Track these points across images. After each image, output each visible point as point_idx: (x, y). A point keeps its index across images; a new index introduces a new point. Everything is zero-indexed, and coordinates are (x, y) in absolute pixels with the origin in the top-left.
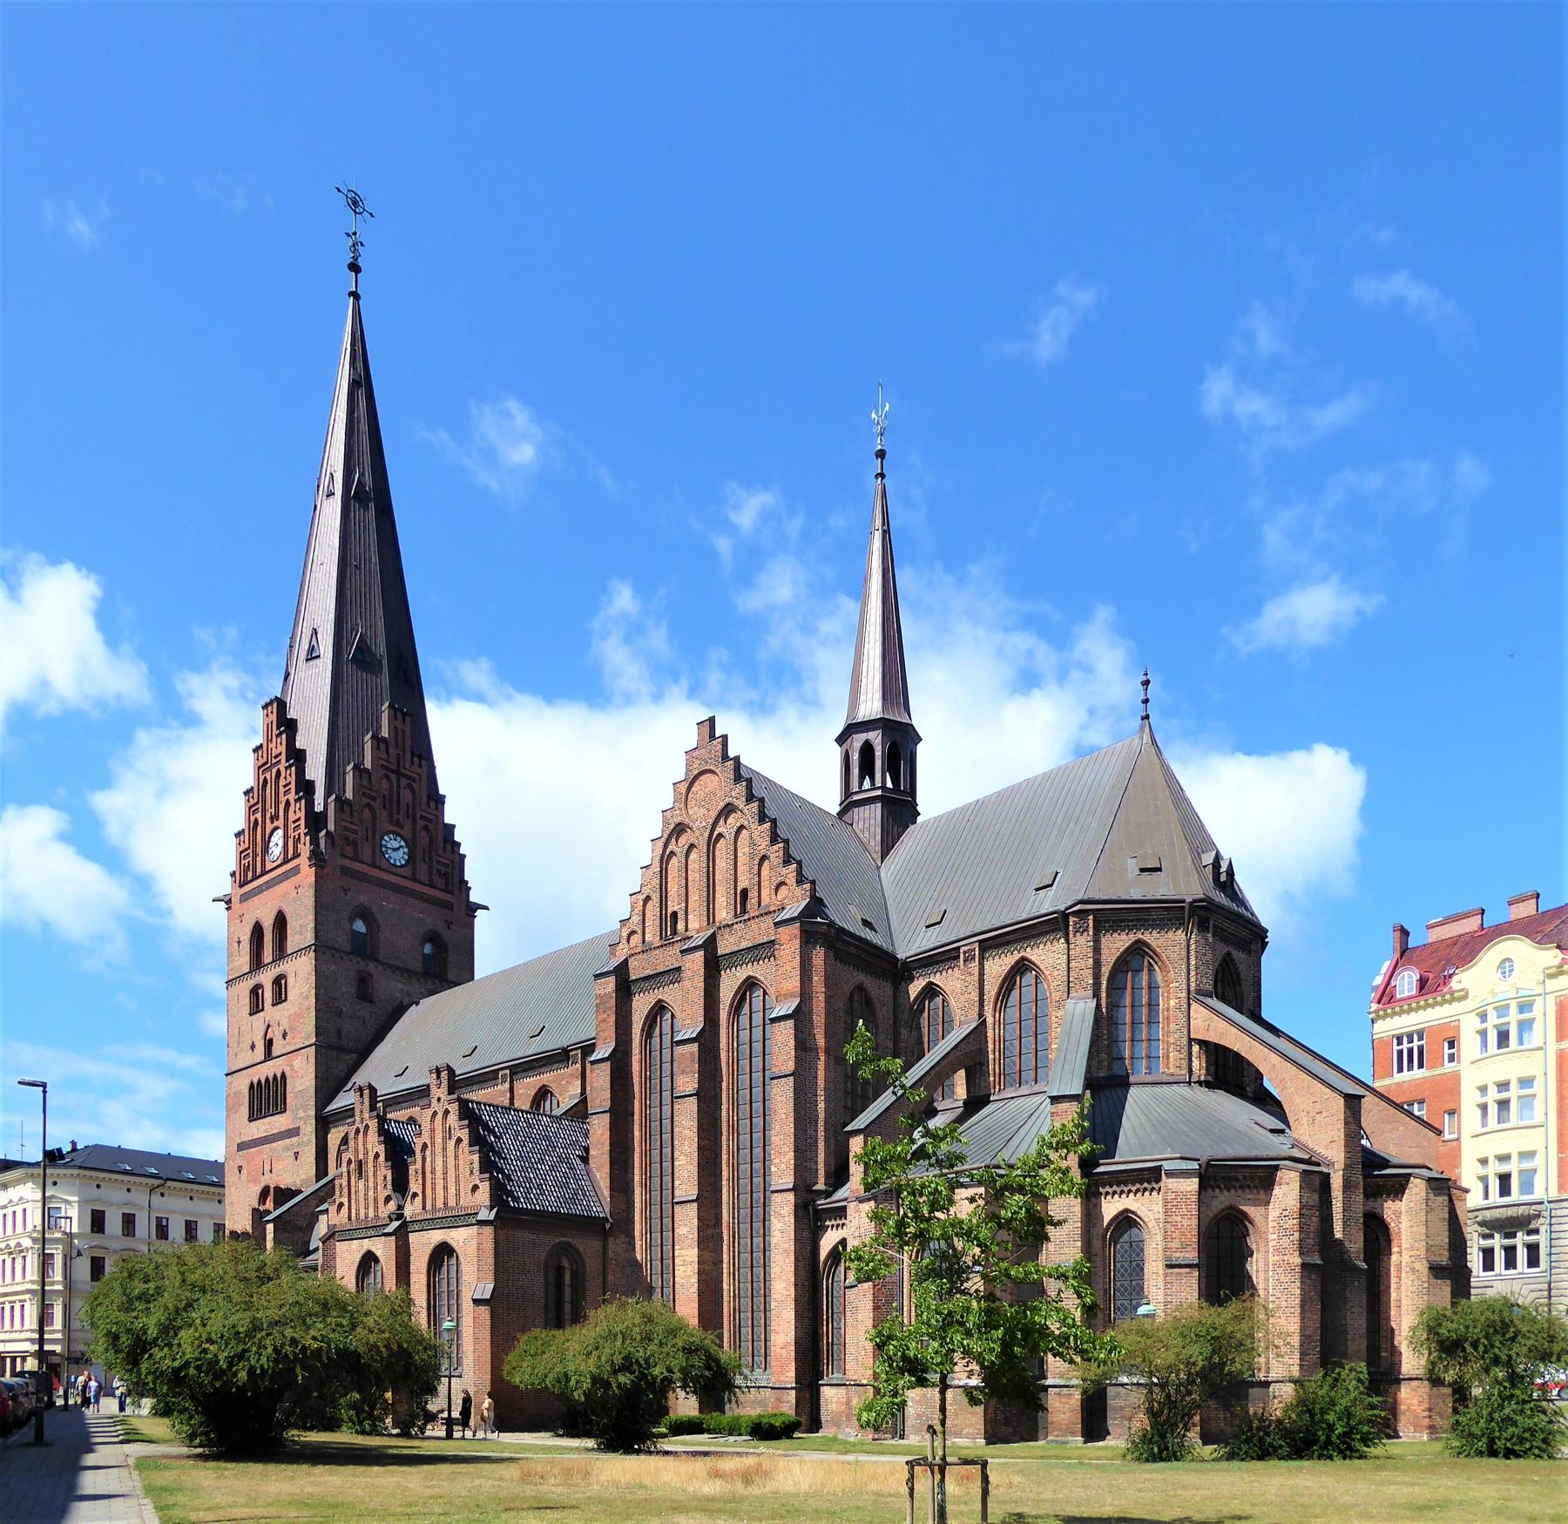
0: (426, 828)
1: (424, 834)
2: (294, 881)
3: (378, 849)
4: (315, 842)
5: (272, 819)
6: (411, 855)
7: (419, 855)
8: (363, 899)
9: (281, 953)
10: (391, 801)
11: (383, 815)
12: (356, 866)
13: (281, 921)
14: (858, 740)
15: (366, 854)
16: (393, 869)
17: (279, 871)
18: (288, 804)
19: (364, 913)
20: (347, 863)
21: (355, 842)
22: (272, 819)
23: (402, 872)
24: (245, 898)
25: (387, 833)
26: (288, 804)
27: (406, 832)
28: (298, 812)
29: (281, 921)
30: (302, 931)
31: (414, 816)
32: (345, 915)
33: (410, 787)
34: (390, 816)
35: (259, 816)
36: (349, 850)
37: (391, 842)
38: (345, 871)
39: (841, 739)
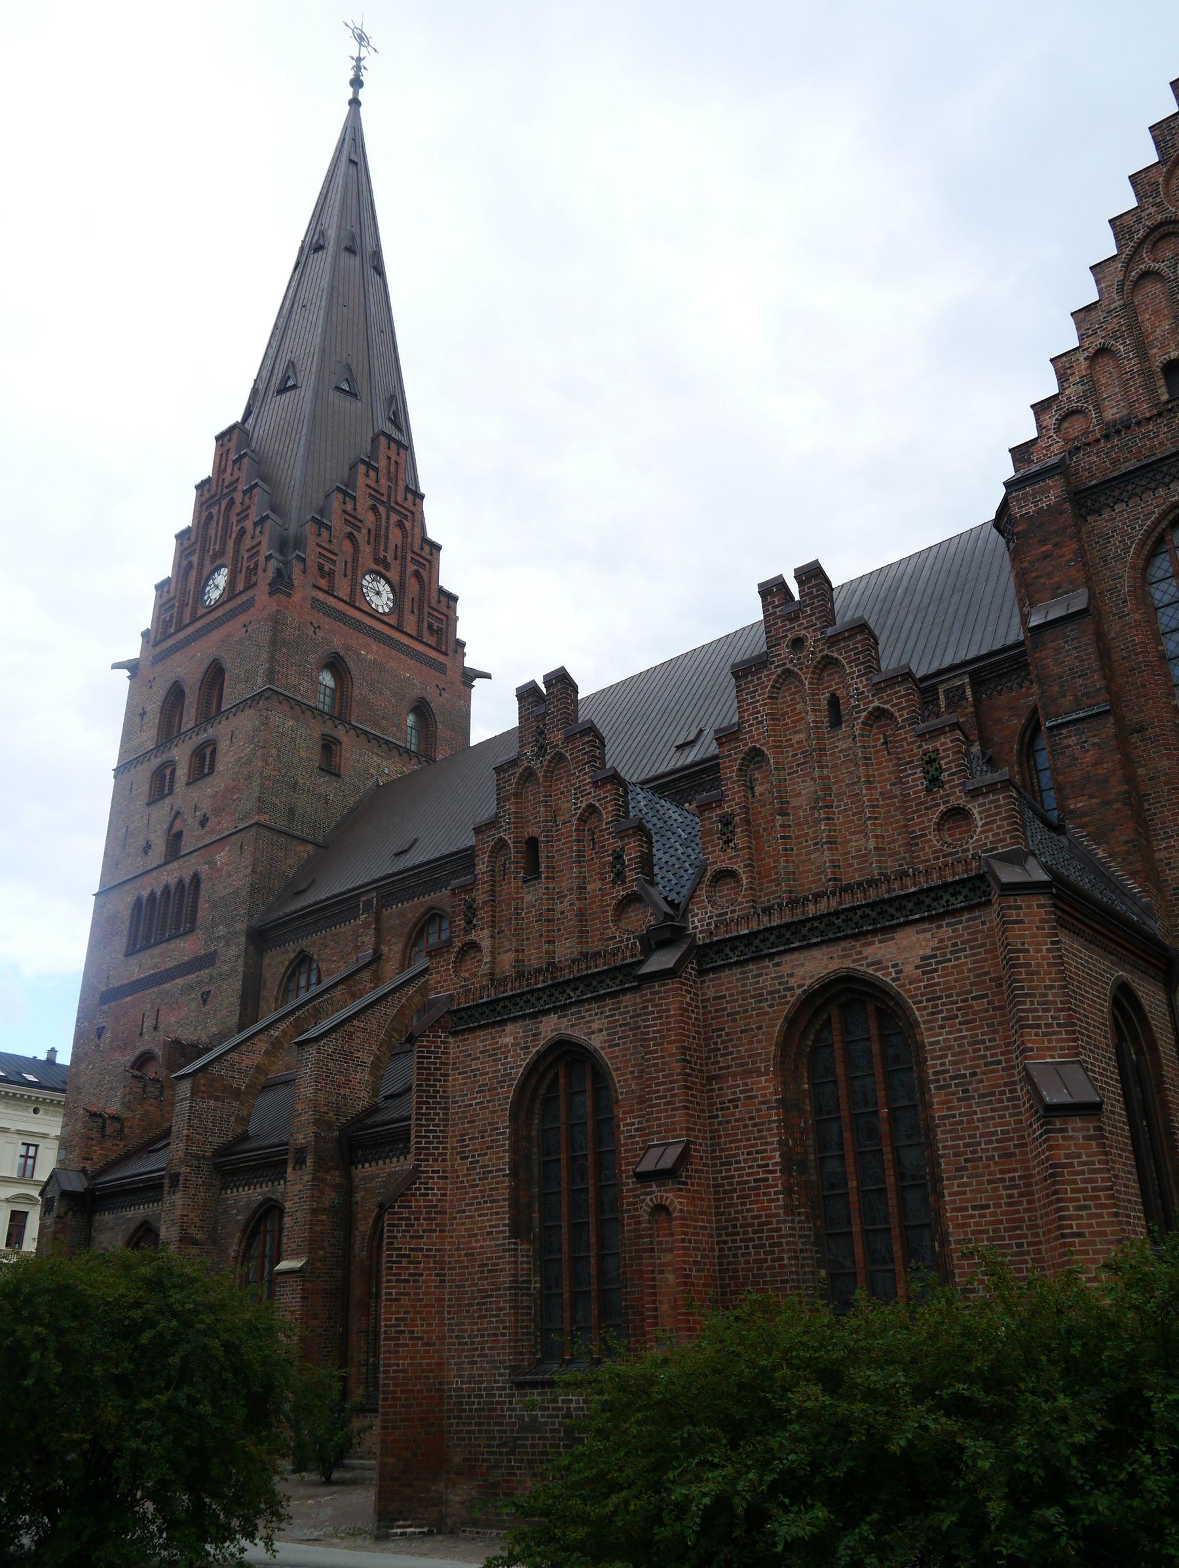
0: (417, 574)
1: (413, 581)
3: (356, 588)
7: (408, 605)
8: (337, 643)
10: (377, 536)
11: (366, 550)
12: (331, 601)
15: (343, 591)
16: (374, 615)
17: (219, 612)
19: (335, 664)
20: (320, 596)
21: (330, 575)
23: (386, 619)
25: (371, 572)
27: (393, 575)
31: (404, 558)
32: (312, 658)
33: (400, 525)
34: (376, 550)
36: (323, 583)
38: (316, 604)
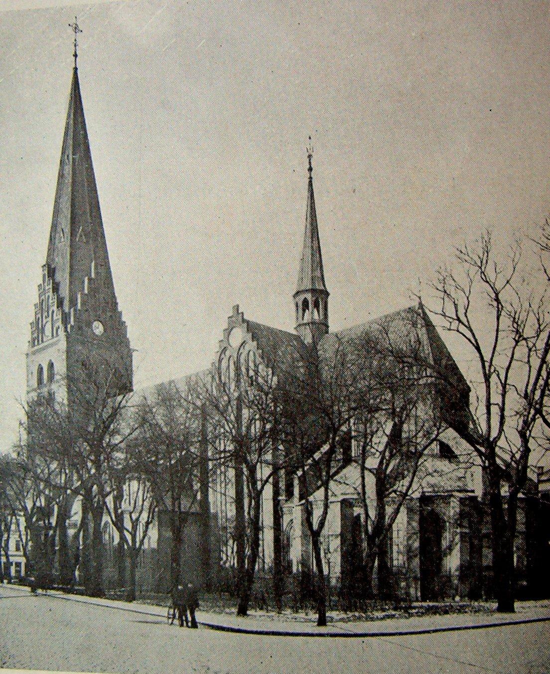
2: (57, 347)
4: (66, 331)
5: (46, 317)
6: (105, 330)
9: (51, 378)
13: (51, 365)
14: (301, 297)
18: (53, 312)
22: (46, 317)
24: (34, 353)
26: (53, 312)
28: (58, 316)
29: (51, 365)
30: (61, 368)
35: (40, 315)
37: (96, 324)
39: (295, 296)
